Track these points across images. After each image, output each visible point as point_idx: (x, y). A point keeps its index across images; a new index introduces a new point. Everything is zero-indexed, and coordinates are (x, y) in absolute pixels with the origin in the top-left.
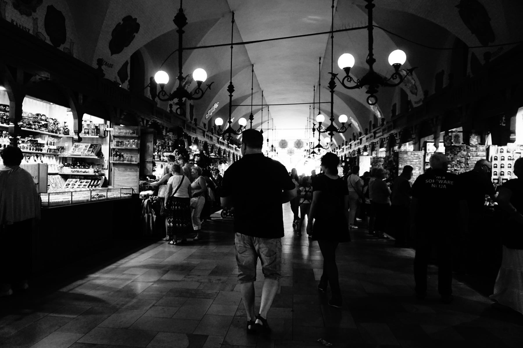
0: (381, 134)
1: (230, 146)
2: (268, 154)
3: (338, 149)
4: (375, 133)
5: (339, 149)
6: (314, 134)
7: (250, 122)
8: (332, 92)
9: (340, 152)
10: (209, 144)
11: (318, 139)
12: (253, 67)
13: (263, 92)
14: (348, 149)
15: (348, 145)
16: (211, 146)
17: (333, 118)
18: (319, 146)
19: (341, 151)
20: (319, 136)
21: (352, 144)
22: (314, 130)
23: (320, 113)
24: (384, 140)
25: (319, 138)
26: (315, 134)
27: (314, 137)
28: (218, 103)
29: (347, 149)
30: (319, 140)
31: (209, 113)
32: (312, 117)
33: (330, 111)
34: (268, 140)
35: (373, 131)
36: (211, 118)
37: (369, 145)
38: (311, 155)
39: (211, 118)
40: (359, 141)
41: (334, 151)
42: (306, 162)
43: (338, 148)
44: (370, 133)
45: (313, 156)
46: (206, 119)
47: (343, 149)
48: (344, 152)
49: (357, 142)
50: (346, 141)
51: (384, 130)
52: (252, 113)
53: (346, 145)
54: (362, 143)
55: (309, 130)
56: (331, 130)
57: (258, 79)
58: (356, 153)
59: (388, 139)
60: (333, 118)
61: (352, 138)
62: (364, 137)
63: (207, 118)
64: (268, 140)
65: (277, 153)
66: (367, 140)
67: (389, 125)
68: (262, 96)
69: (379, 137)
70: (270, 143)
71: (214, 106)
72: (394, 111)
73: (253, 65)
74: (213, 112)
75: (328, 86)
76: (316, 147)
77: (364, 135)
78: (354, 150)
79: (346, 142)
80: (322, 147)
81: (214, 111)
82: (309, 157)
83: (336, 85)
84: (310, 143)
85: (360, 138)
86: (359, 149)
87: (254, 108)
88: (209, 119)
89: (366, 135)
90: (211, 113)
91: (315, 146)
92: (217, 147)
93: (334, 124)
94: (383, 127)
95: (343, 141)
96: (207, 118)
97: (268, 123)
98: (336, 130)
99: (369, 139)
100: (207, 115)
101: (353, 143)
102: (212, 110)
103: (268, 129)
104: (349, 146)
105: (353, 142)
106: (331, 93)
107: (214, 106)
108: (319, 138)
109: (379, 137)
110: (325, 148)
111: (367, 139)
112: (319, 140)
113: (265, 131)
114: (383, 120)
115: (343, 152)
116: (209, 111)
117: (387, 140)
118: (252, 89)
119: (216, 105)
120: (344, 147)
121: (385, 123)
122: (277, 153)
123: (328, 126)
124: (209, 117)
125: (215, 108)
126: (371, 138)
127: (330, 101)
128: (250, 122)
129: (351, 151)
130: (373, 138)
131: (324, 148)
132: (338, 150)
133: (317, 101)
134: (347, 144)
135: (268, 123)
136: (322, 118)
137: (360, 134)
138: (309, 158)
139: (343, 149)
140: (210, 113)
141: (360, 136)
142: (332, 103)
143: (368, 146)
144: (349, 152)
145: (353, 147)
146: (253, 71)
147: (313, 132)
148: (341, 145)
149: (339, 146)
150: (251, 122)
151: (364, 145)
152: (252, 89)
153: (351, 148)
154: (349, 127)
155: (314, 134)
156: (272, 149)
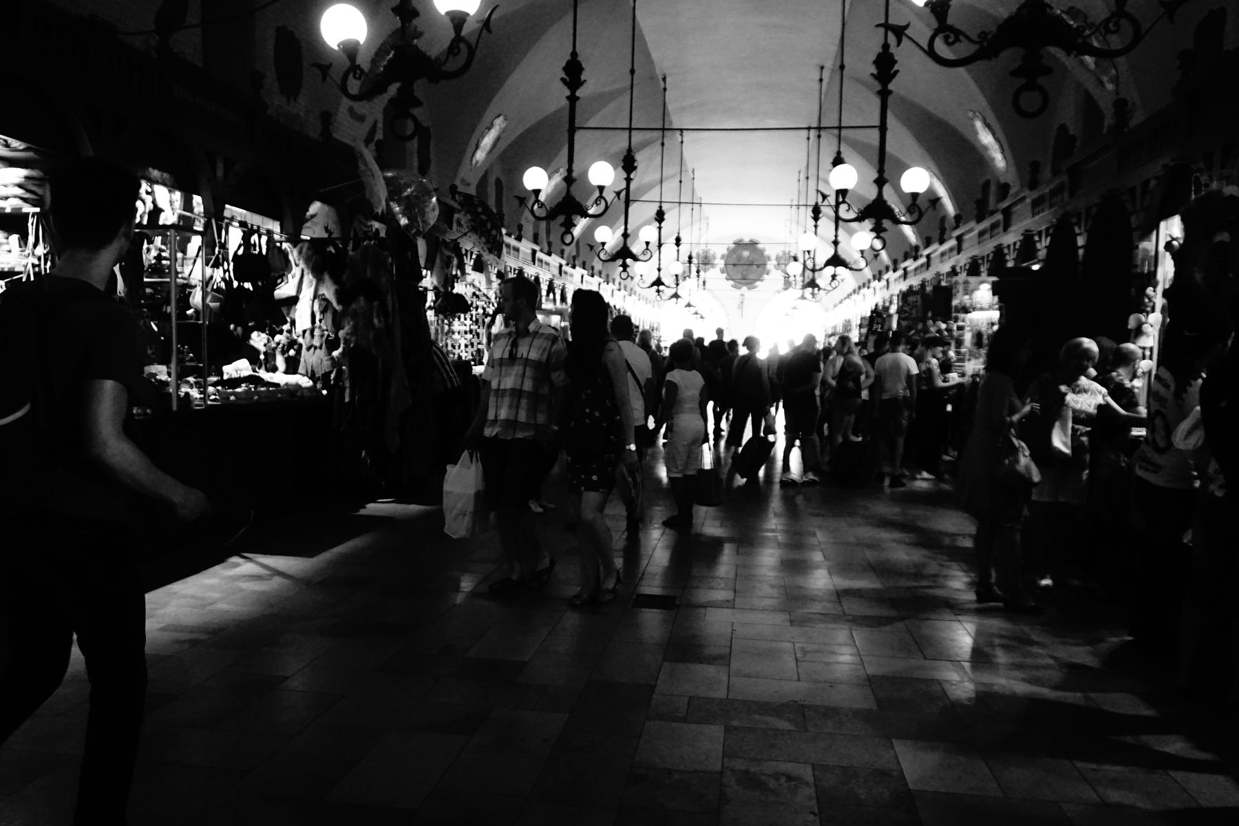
3: (891, 272)
5: (879, 280)
6: (816, 226)
7: (625, 179)
8: (884, 94)
9: (896, 280)
11: (834, 238)
15: (921, 256)
19: (900, 277)
20: (836, 229)
21: (932, 256)
23: (838, 161)
25: (836, 236)
26: (818, 228)
27: (816, 233)
29: (916, 269)
30: (836, 243)
32: (813, 171)
34: (678, 241)
41: (878, 277)
43: (891, 268)
45: (834, 277)
47: (887, 281)
48: (930, 269)
52: (630, 150)
53: (915, 259)
55: (802, 209)
64: (678, 241)
65: (704, 283)
70: (685, 250)
75: (872, 74)
78: (938, 274)
80: (844, 264)
82: (803, 297)
83: (897, 72)
84: (804, 252)
85: (957, 233)
87: (637, 137)
91: (821, 261)
93: (888, 194)
97: (681, 182)
101: (936, 249)
103: (680, 203)
105: (935, 246)
108: (836, 236)
110: (854, 267)
112: (836, 243)
113: (670, 209)
115: (927, 269)
120: (910, 264)
122: (704, 283)
123: (868, 203)
127: (877, 122)
128: (625, 179)
129: (928, 275)
132: (890, 275)
133: (830, 120)
134: (919, 253)
135: (681, 182)
136: (847, 176)
138: (800, 301)
139: (887, 281)
142: (883, 128)
148: (900, 258)
149: (895, 262)
150: (628, 180)
155: (816, 226)
156: (690, 267)
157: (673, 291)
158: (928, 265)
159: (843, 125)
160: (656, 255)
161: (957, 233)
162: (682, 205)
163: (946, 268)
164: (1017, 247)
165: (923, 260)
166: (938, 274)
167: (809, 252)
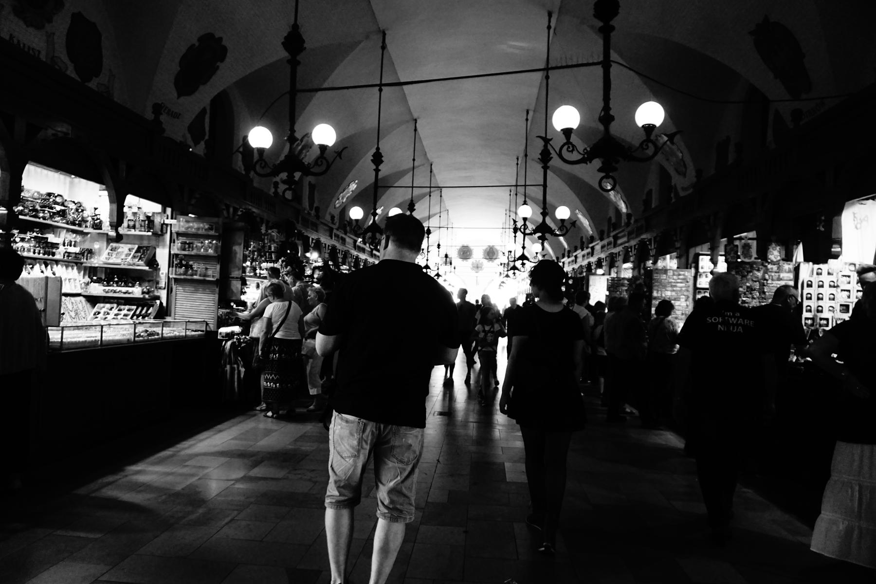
0: (625, 239)
1: (375, 255)
2: (438, 269)
4: (616, 238)
6: (515, 237)
8: (545, 168)
10: (339, 250)
12: (416, 123)
13: (431, 165)
14: (571, 264)
15: (573, 256)
16: (343, 253)
17: (546, 210)
18: (523, 257)
21: (578, 256)
22: (516, 230)
23: (525, 203)
24: (630, 250)
25: (524, 244)
26: (516, 238)
28: (356, 181)
29: (569, 263)
30: (524, 248)
31: (340, 199)
32: (513, 209)
33: (541, 198)
34: (439, 246)
35: (612, 234)
36: (345, 206)
37: (606, 258)
38: (511, 273)
39: (343, 206)
40: (589, 250)
42: (502, 284)
44: (608, 236)
45: (514, 273)
46: (335, 208)
49: (586, 252)
50: (569, 249)
51: (630, 234)
52: (412, 201)
53: (569, 257)
54: (595, 253)
56: (543, 231)
57: (424, 143)
58: (585, 270)
59: (636, 249)
60: (546, 210)
61: (579, 246)
62: (597, 244)
63: (337, 206)
64: (439, 246)
65: (455, 268)
66: (603, 250)
67: (639, 224)
68: (431, 172)
69: (621, 244)
70: (443, 251)
71: (349, 186)
72: (647, 202)
73: (416, 120)
74: (348, 197)
75: (539, 159)
76: (519, 259)
77: (598, 240)
78: (581, 266)
79: (569, 252)
80: (527, 259)
81: (349, 194)
82: (507, 276)
83: (552, 158)
85: (591, 245)
86: (589, 264)
87: (417, 192)
88: (341, 208)
89: (601, 241)
90: (344, 197)
91: (517, 256)
92: (354, 256)
93: (548, 221)
94: (629, 229)
95: (565, 249)
96: (337, 206)
97: (440, 217)
98: (552, 232)
99: (606, 249)
100: (337, 202)
101: (580, 253)
102: (347, 194)
103: (440, 227)
104: (573, 258)
105: (579, 251)
106: (543, 170)
107: (350, 187)
108: (524, 244)
109: (621, 244)
111: (603, 247)
112: (524, 248)
113: (435, 231)
114: (629, 216)
116: (341, 195)
117: (636, 251)
118: (414, 160)
119: (354, 185)
121: (632, 221)
122: (455, 268)
124: (340, 206)
125: (351, 190)
126: (609, 247)
129: (576, 266)
130: (612, 246)
131: (531, 262)
134: (570, 255)
135: (440, 217)
137: (592, 239)
138: (506, 278)
140: (343, 198)
141: (592, 242)
142: (545, 186)
143: (603, 259)
144: (573, 269)
145: (580, 260)
146: (416, 130)
147: (514, 235)
148: (560, 256)
151: (597, 257)
152: (414, 160)
153: (576, 262)
154: (573, 227)
155: (515, 237)
157: (436, 272)
158: (575, 261)
159: (524, 187)
160: (426, 256)
161: (574, 254)
162: (441, 229)
163: (585, 263)
164: (636, 247)
165: (573, 258)
166: (581, 266)
167: (511, 252)
